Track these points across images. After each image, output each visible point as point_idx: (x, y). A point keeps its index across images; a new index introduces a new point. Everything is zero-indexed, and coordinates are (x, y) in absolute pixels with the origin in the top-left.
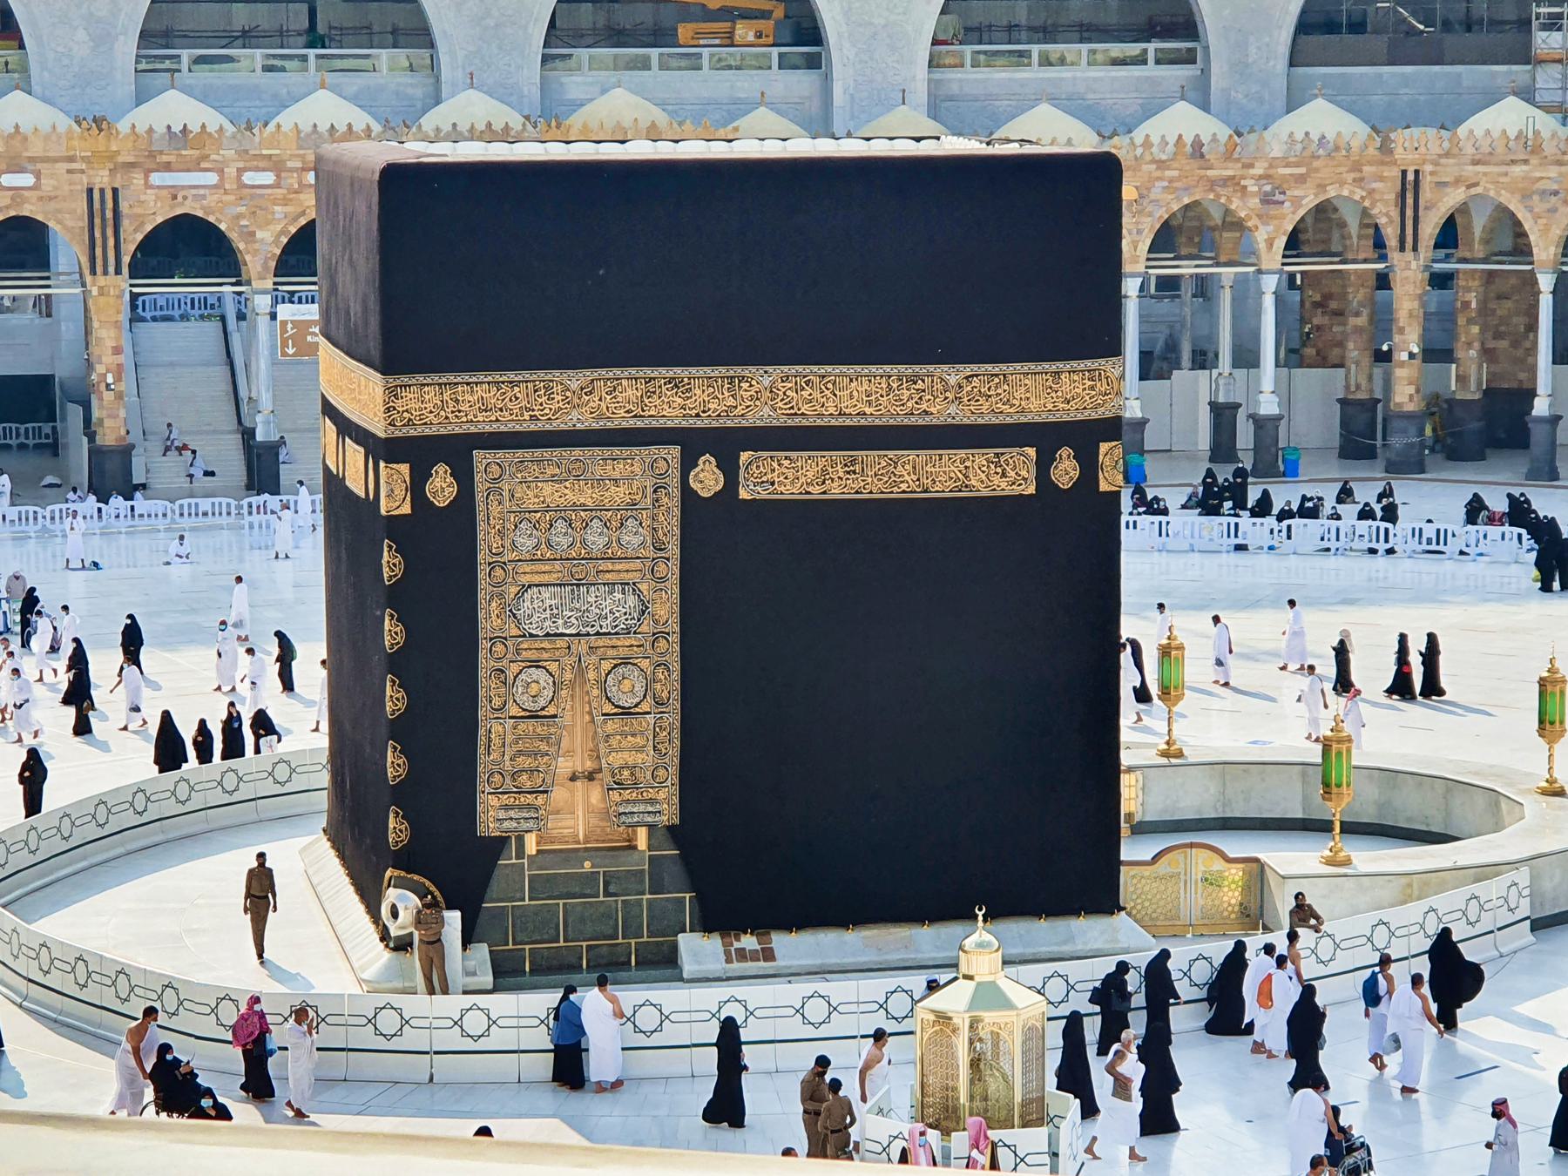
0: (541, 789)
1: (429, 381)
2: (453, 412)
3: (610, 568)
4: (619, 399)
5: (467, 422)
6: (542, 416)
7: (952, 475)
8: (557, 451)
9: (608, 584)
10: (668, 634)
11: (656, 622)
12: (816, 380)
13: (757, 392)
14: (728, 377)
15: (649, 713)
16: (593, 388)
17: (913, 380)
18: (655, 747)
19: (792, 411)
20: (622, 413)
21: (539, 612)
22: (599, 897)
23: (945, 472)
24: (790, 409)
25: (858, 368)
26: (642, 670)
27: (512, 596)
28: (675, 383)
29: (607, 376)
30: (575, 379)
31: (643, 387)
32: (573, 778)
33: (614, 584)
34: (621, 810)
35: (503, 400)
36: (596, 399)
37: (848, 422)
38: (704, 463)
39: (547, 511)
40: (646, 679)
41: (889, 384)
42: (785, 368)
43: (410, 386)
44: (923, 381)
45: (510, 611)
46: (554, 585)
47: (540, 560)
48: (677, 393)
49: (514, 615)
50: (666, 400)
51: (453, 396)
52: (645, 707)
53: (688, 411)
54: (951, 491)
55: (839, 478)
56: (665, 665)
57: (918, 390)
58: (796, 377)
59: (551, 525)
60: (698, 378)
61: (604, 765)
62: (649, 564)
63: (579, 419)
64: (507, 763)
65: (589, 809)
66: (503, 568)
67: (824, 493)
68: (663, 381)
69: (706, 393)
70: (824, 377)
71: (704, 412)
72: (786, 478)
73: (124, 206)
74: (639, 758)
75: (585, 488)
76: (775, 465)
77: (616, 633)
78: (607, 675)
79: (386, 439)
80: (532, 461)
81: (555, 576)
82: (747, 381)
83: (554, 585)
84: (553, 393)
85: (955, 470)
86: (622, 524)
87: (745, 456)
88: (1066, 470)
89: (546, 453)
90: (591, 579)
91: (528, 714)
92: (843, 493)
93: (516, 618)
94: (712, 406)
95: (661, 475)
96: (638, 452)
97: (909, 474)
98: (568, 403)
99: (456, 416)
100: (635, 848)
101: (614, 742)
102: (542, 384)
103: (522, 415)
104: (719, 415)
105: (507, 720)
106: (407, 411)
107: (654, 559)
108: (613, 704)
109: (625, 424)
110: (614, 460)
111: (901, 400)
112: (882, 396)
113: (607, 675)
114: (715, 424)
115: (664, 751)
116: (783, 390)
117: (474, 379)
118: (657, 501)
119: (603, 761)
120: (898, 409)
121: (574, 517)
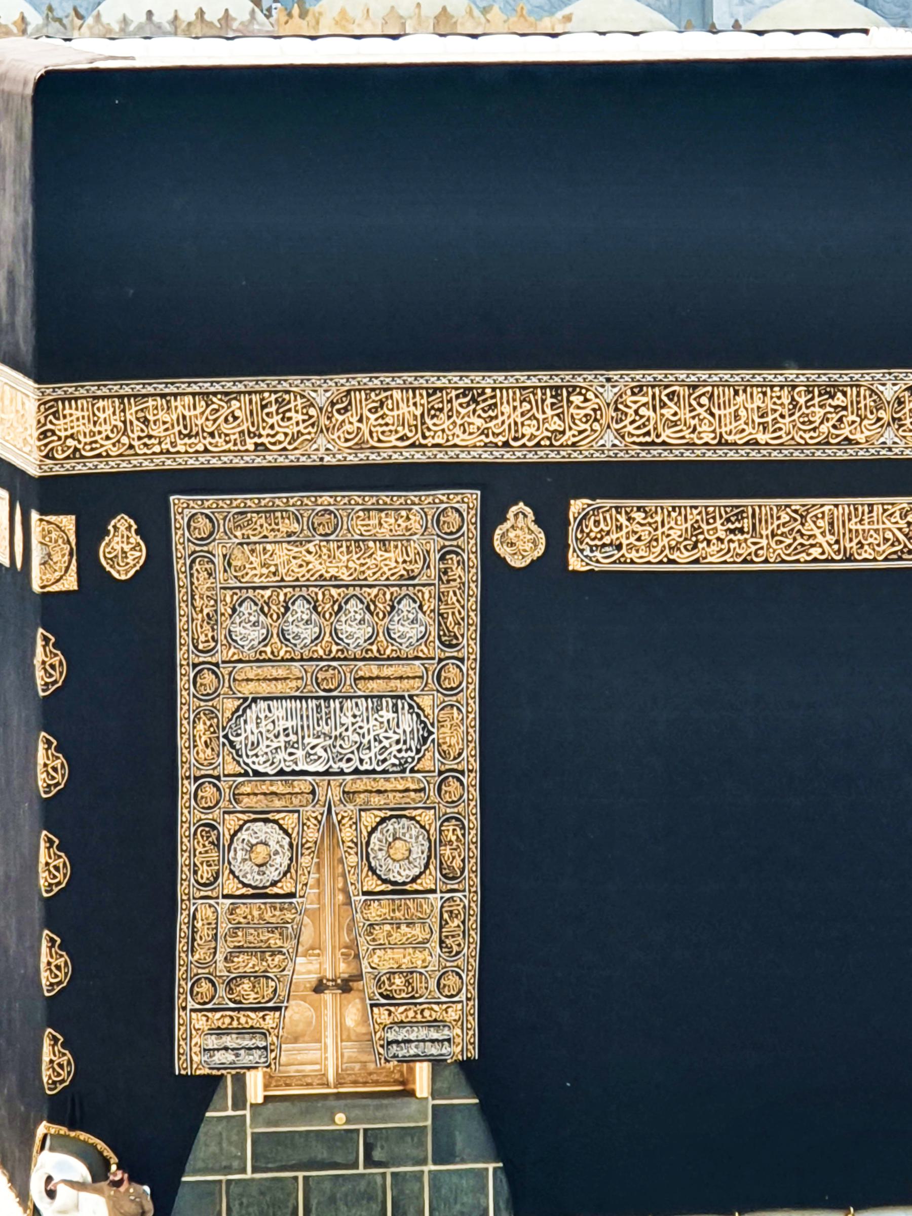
0: (270, 1004)
1: (105, 391)
2: (140, 438)
3: (375, 672)
4: (389, 420)
5: (161, 453)
6: (274, 444)
7: (889, 535)
8: (295, 497)
9: (372, 697)
10: (462, 773)
11: (444, 755)
12: (683, 391)
13: (594, 410)
14: (551, 388)
15: (433, 891)
16: (350, 404)
17: (830, 391)
18: (441, 942)
19: (648, 439)
20: (393, 440)
22: (357, 1168)
23: (877, 531)
24: (644, 435)
25: (746, 374)
26: (423, 827)
27: (228, 714)
28: (473, 396)
29: (371, 385)
31: (424, 401)
32: (319, 988)
33: (380, 697)
34: (391, 1036)
35: (215, 420)
36: (354, 419)
37: (732, 456)
38: (516, 515)
39: (280, 587)
40: (430, 841)
41: (793, 399)
42: (638, 374)
43: (76, 399)
44: (844, 394)
45: (226, 736)
46: (291, 698)
47: (270, 660)
48: (474, 411)
49: (231, 743)
50: (459, 422)
51: (140, 415)
52: (427, 882)
53: (491, 438)
54: (886, 559)
55: (718, 539)
56: (457, 819)
57: (836, 407)
58: (653, 387)
59: (287, 609)
60: (507, 389)
61: (366, 969)
62: (433, 666)
64: (221, 965)
65: (343, 1034)
66: (214, 672)
67: (696, 561)
68: (454, 393)
69: (519, 411)
70: (695, 387)
71: (516, 439)
72: (639, 539)
74: (418, 959)
75: (337, 554)
76: (623, 519)
77: (384, 772)
78: (370, 834)
79: (41, 477)
80: (258, 513)
81: (294, 684)
82: (580, 394)
83: (291, 698)
84: (289, 410)
86: (393, 608)
87: (577, 506)
89: (279, 499)
90: (346, 690)
91: (251, 891)
92: (725, 562)
93: (233, 747)
94: (527, 431)
95: (452, 533)
96: (416, 500)
97: (823, 534)
98: (313, 425)
99: (145, 445)
100: (411, 1094)
101: (380, 933)
102: (273, 397)
103: (244, 443)
104: (538, 445)
105: (221, 901)
106: (72, 436)
107: (440, 660)
108: (379, 877)
109: (397, 458)
110: (381, 510)
111: (811, 422)
112: (782, 416)
113: (370, 834)
114: (532, 458)
115: (455, 948)
116: (635, 407)
117: (172, 389)
118: (445, 573)
119: (365, 963)
120: (807, 436)
121: (320, 597)
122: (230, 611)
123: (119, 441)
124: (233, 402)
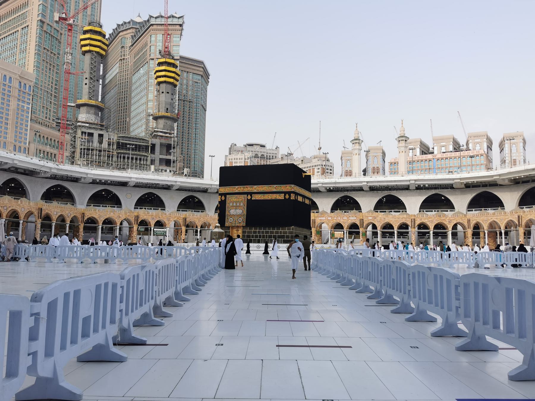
21: (233, 212)
30: (237, 187)
63: (237, 191)
73: (316, 221)
85: (275, 196)
88: (287, 196)
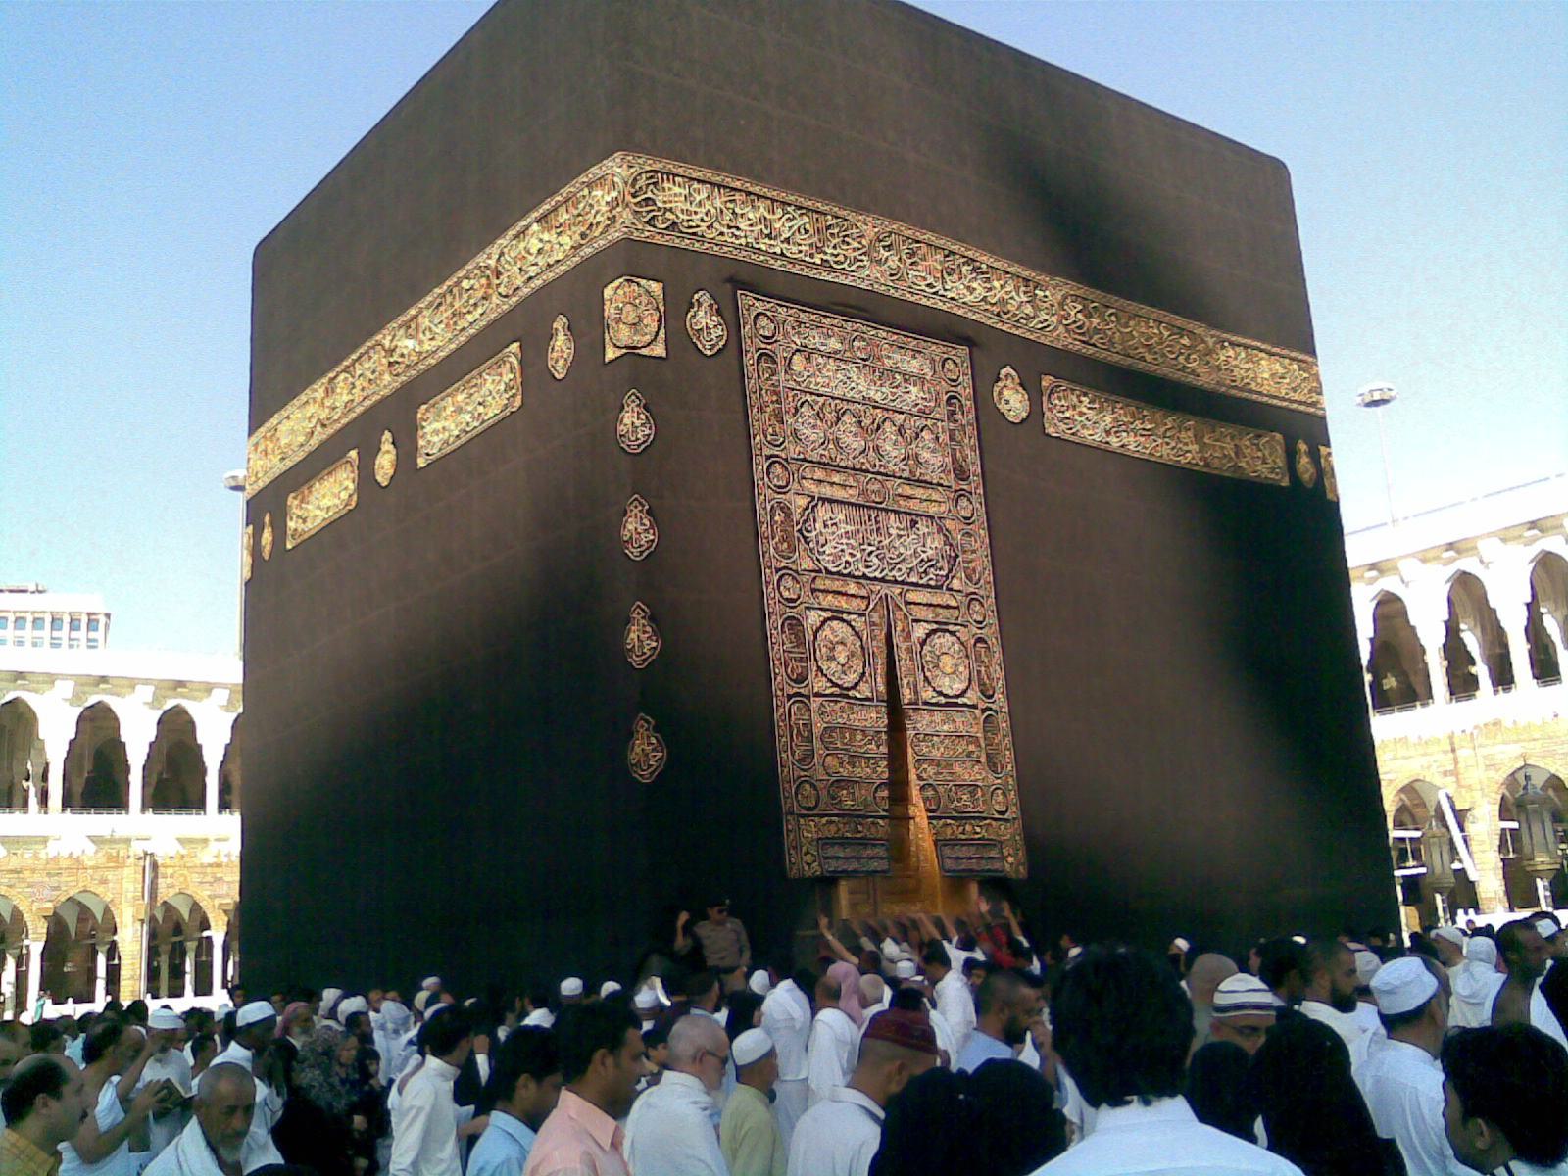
4: (920, 267)
43: (675, 175)
117: (756, 189)
122: (793, 411)
123: (712, 225)
124: (804, 217)
